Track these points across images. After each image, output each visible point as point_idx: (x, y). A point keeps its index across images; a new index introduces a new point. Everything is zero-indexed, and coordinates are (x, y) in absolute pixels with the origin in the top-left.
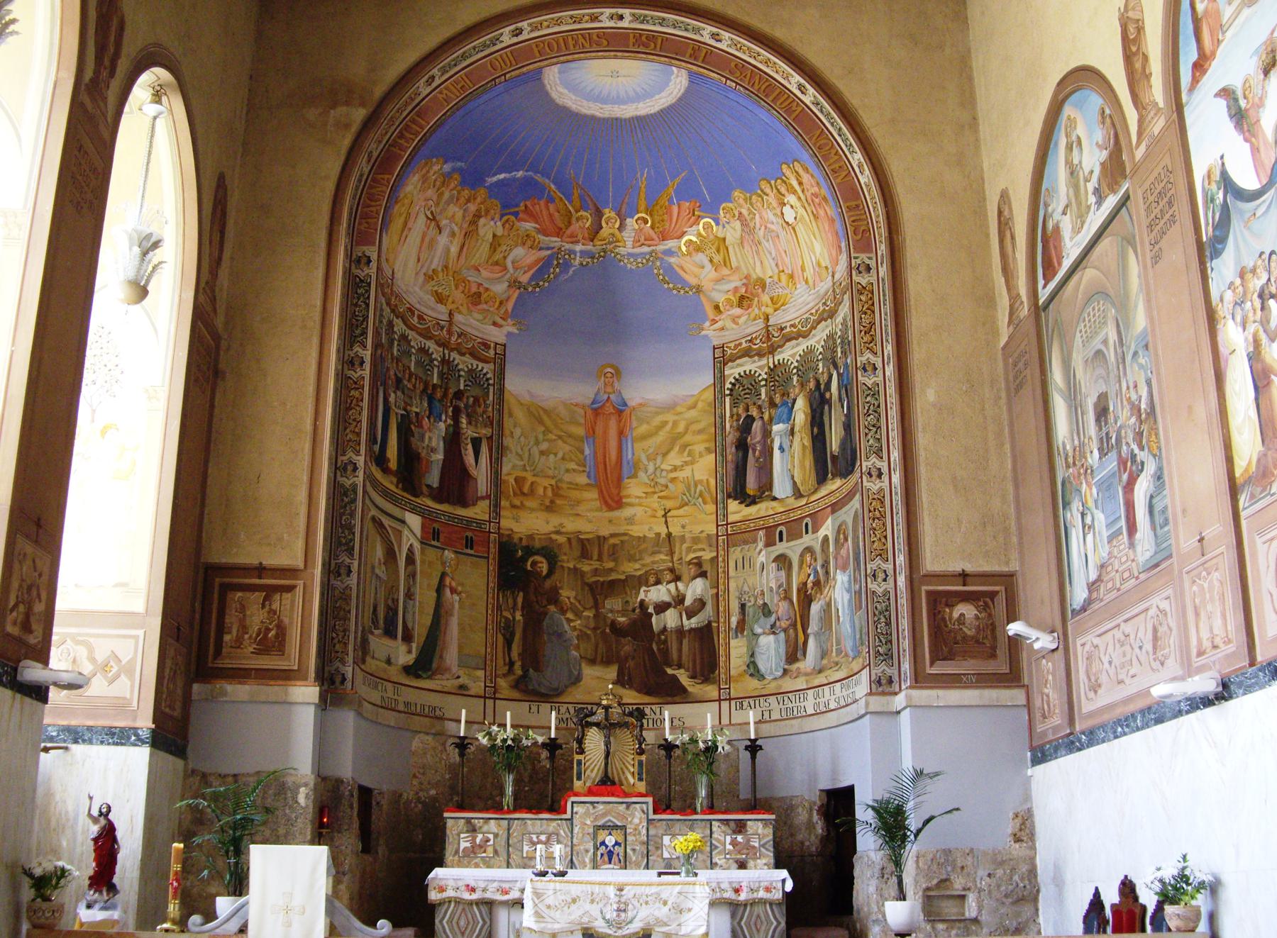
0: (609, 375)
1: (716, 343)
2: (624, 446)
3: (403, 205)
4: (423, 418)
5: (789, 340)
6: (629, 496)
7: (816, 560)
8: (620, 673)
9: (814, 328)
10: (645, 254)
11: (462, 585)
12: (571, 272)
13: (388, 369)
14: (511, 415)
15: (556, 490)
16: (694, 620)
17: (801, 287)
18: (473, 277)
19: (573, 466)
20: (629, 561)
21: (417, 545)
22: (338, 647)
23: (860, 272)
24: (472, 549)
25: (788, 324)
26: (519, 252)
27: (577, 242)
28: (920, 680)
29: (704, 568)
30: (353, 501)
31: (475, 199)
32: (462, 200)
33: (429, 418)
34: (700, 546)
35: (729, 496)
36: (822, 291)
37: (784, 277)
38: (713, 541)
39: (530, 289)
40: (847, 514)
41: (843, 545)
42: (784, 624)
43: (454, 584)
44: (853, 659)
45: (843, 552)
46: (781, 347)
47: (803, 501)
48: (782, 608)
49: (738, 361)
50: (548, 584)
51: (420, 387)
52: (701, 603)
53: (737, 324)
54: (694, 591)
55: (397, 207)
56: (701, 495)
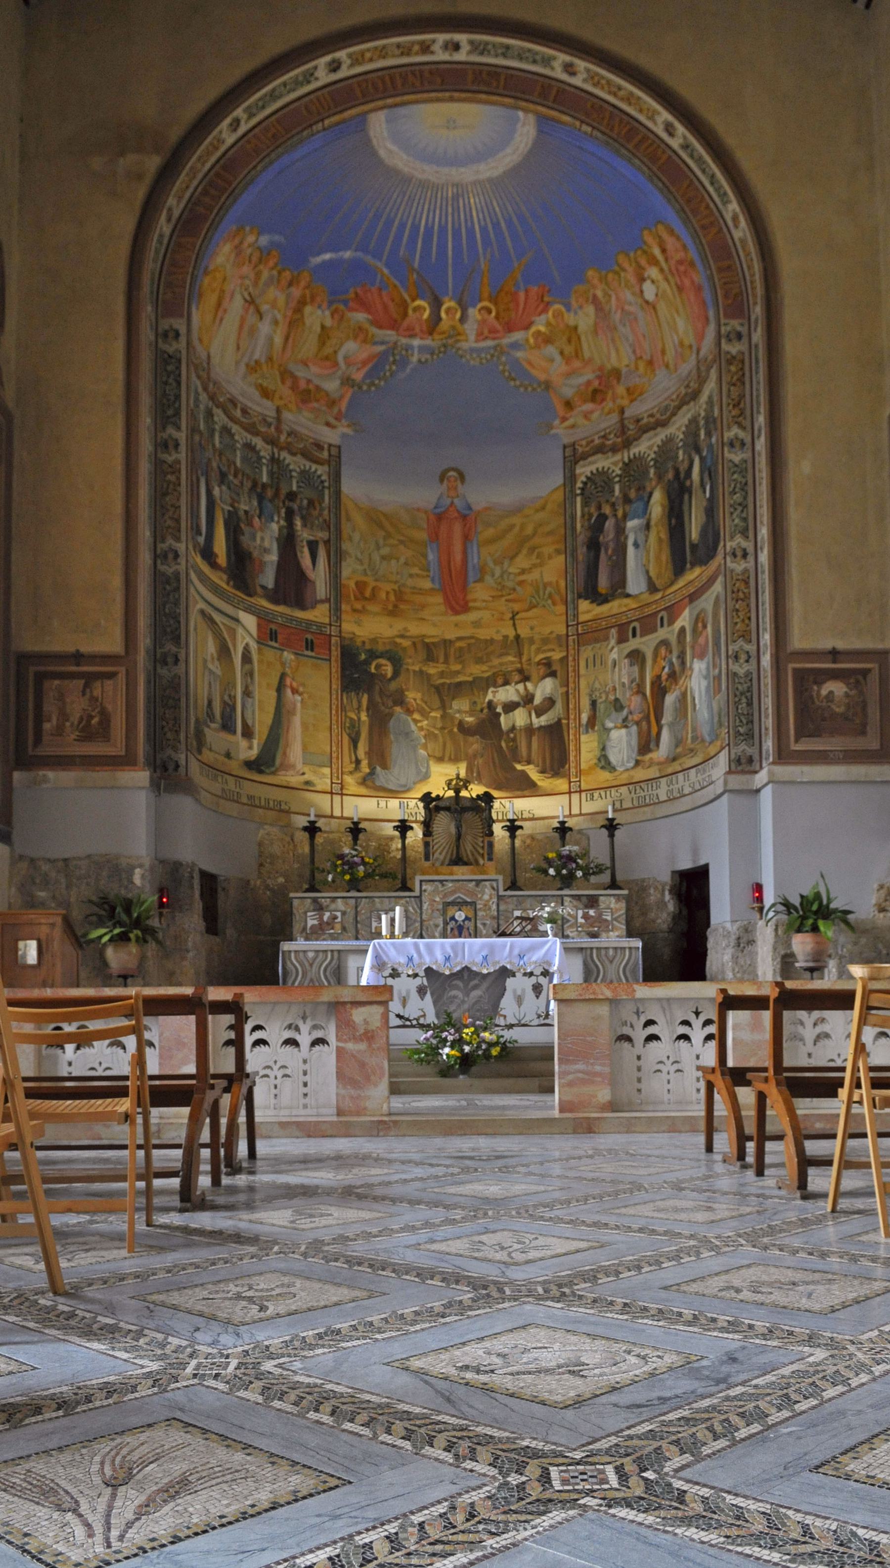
6: (475, 600)
7: (671, 652)
10: (489, 348)
14: (348, 519)
19: (415, 570)
21: (254, 646)
24: (312, 650)
28: (783, 756)
35: (580, 596)
44: (710, 743)
56: (550, 596)
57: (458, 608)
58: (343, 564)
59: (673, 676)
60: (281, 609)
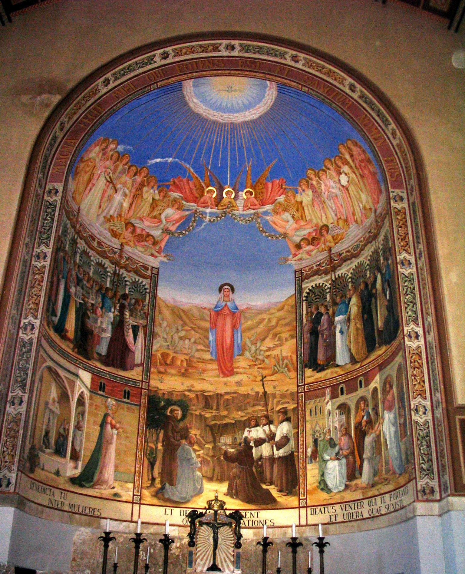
0: (226, 290)
1: (296, 268)
2: (236, 337)
3: (88, 166)
4: (97, 308)
5: (345, 261)
6: (238, 368)
7: (368, 405)
8: (230, 487)
9: (362, 250)
10: (251, 214)
11: (120, 422)
12: (203, 226)
13: (70, 270)
14: (160, 313)
15: (189, 363)
16: (281, 451)
17: (353, 226)
18: (138, 225)
19: (201, 347)
20: (238, 410)
21: (87, 394)
22: (7, 458)
23: (396, 201)
24: (128, 398)
25: (344, 251)
26: (169, 211)
27: (208, 207)
29: (289, 415)
30: (30, 351)
31: (140, 174)
32: (132, 173)
33: (102, 308)
34: (287, 400)
35: (306, 366)
36: (368, 225)
37: (341, 223)
38: (294, 396)
39: (176, 235)
40: (392, 370)
41: (389, 392)
42: (345, 452)
43: (114, 422)
45: (389, 397)
46: (340, 266)
47: (358, 365)
48: (344, 441)
49: (311, 279)
50: (181, 425)
51: (96, 288)
52: (286, 439)
53: (310, 255)
54: (282, 431)
55: (82, 165)
56: (287, 366)
57: (227, 372)
58: (155, 341)
59: (370, 423)
60: (108, 369)
